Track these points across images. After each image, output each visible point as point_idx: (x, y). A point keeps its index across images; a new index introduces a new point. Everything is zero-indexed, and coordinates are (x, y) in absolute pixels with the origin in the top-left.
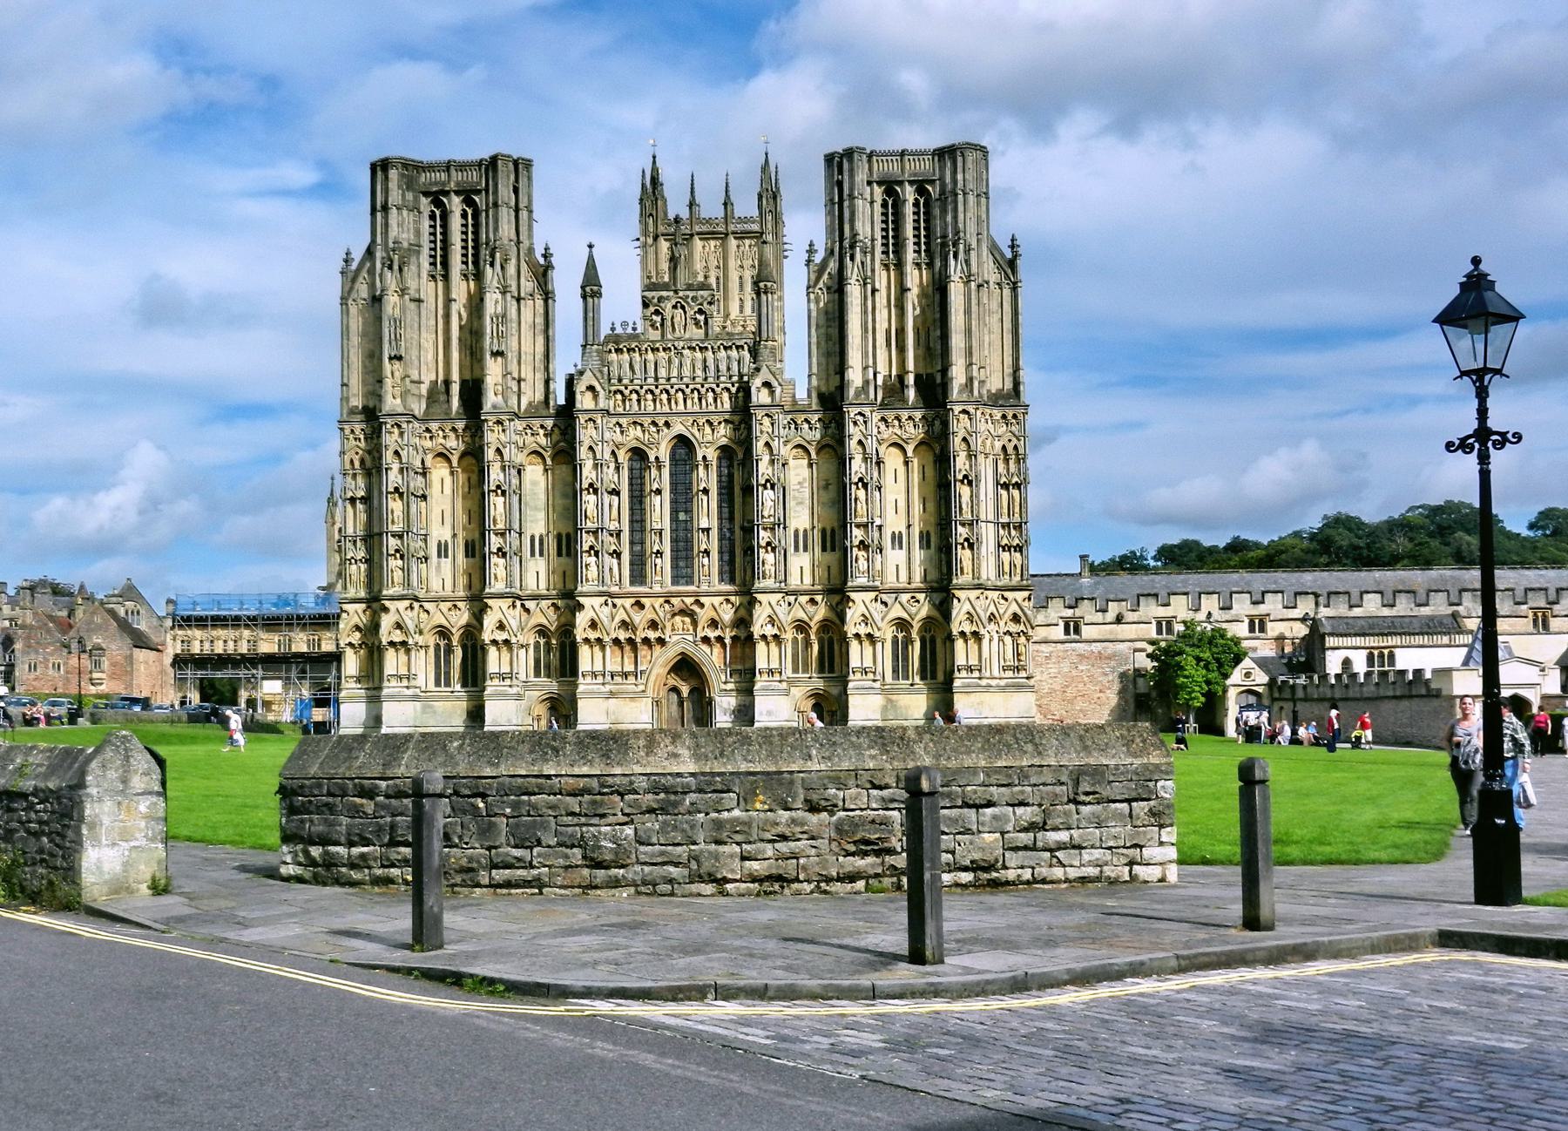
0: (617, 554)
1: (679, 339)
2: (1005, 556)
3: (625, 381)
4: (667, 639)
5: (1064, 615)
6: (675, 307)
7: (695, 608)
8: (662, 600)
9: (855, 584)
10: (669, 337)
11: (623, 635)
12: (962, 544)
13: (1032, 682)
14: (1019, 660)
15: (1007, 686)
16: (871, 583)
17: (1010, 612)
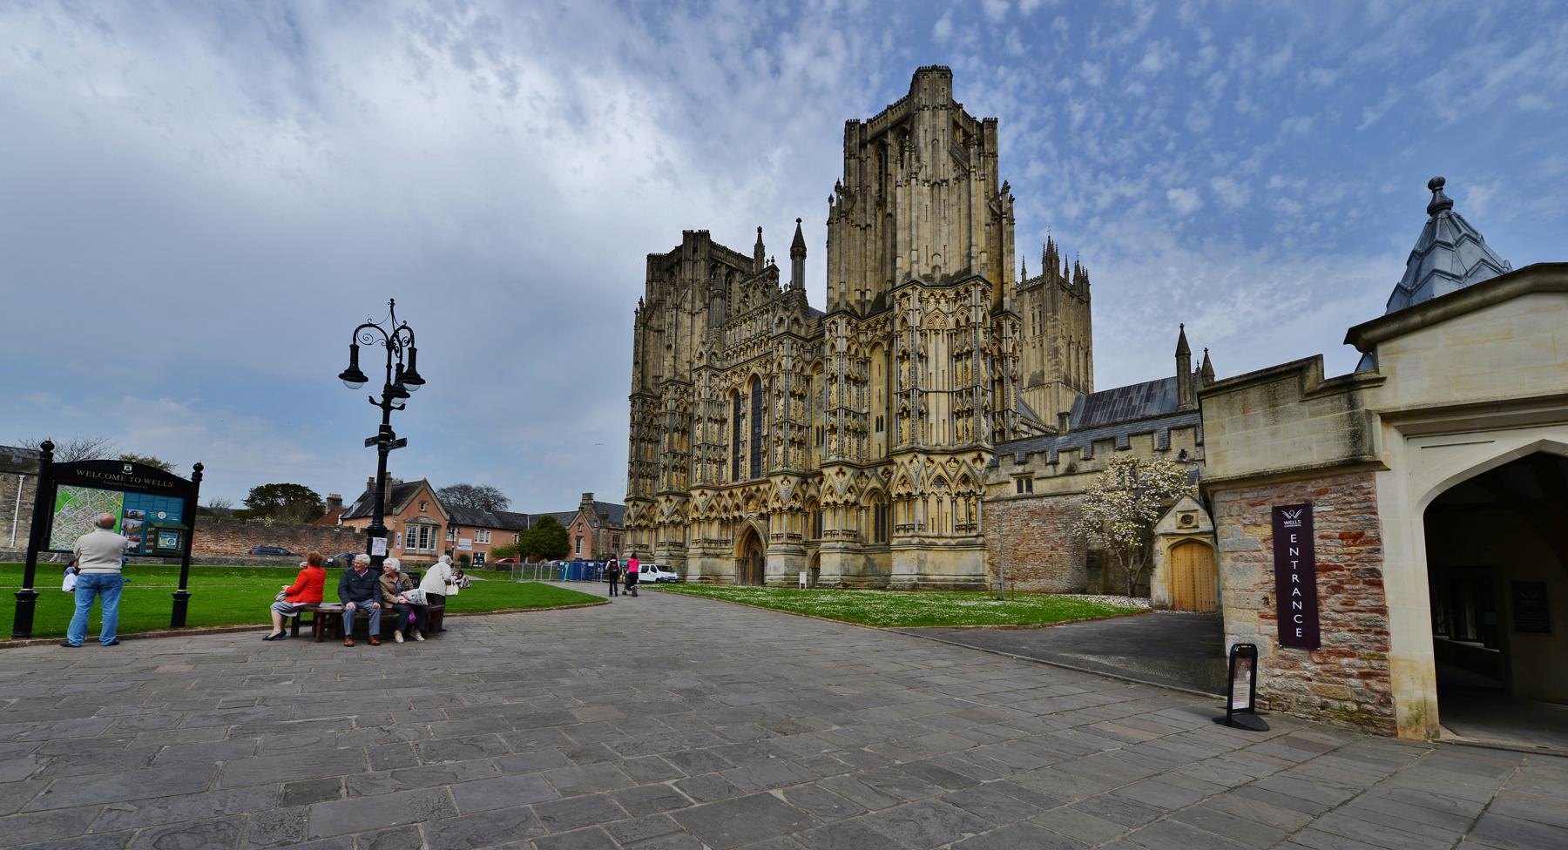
0: (725, 461)
1: (756, 309)
2: (960, 423)
3: (731, 347)
4: (744, 516)
5: (1014, 471)
6: (755, 289)
7: (759, 495)
8: (741, 490)
9: (827, 461)
10: (751, 309)
11: (724, 516)
12: (902, 414)
13: (980, 540)
14: (970, 520)
15: (958, 544)
16: (837, 459)
17: (960, 473)
